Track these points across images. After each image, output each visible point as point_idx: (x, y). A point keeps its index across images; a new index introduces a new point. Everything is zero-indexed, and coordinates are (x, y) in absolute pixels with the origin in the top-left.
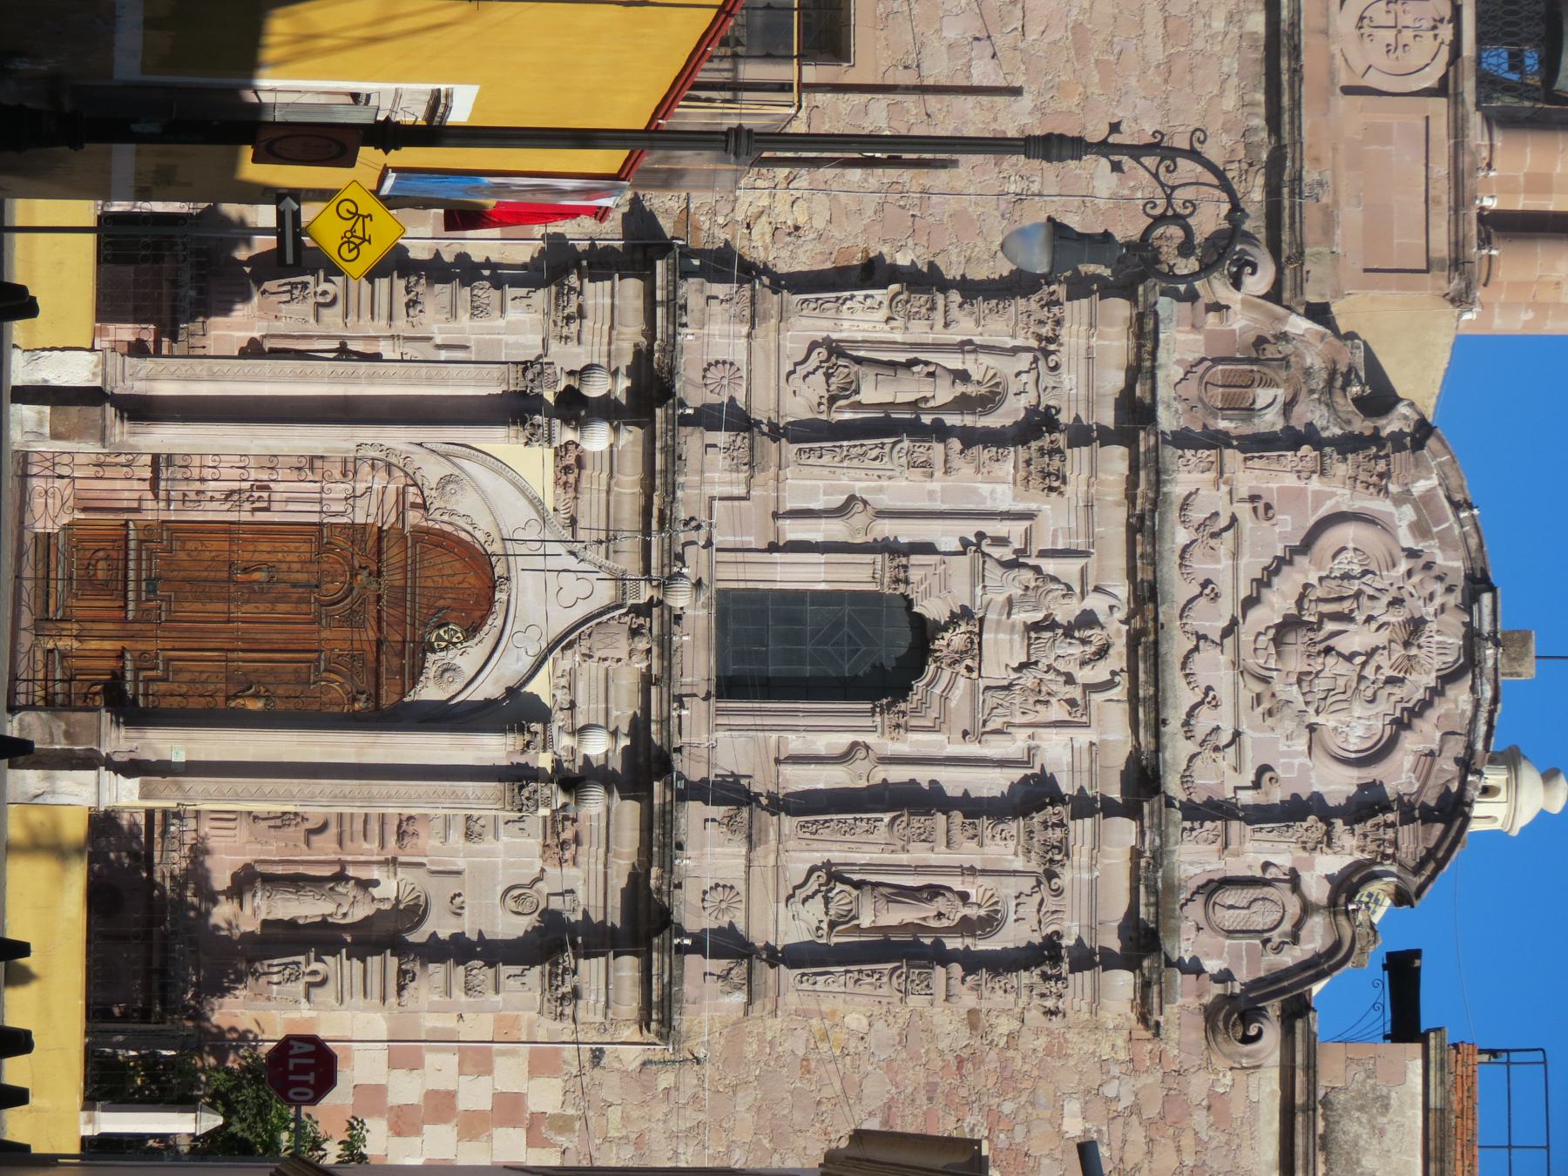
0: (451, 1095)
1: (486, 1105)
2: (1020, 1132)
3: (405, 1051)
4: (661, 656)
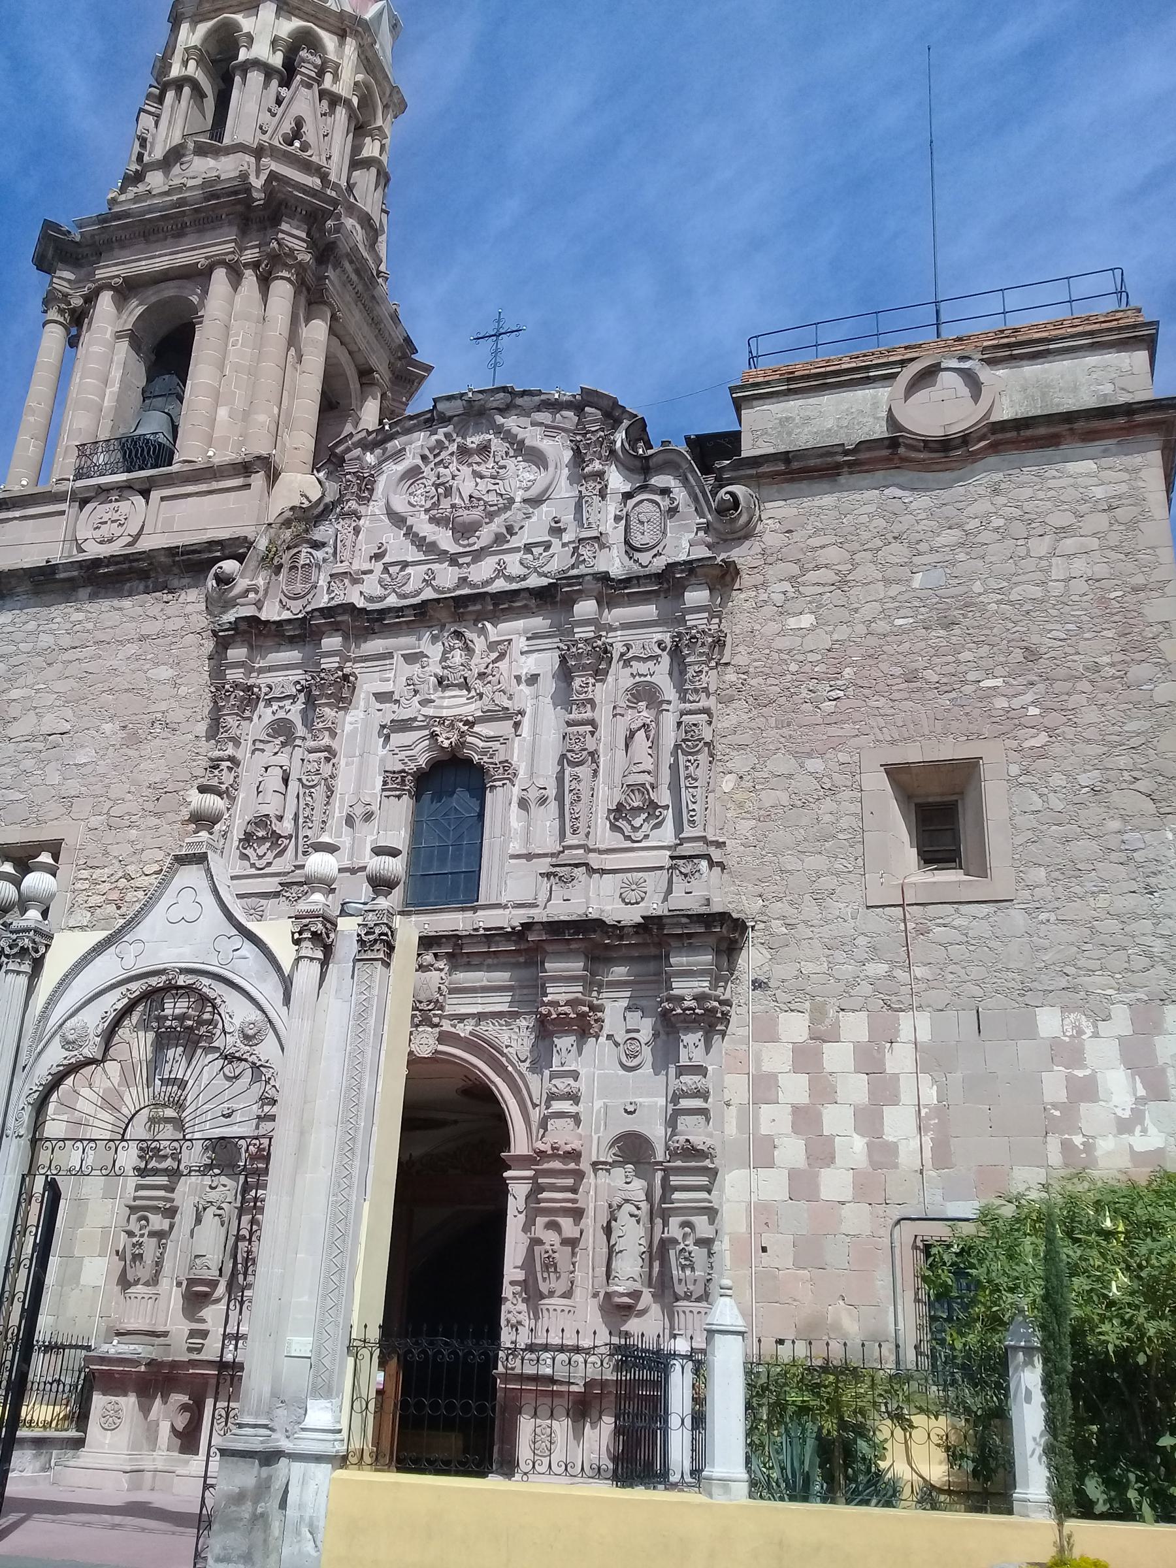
0: (796, 1110)
1: (804, 1079)
2: (812, 657)
3: (762, 1154)
4: (439, 945)
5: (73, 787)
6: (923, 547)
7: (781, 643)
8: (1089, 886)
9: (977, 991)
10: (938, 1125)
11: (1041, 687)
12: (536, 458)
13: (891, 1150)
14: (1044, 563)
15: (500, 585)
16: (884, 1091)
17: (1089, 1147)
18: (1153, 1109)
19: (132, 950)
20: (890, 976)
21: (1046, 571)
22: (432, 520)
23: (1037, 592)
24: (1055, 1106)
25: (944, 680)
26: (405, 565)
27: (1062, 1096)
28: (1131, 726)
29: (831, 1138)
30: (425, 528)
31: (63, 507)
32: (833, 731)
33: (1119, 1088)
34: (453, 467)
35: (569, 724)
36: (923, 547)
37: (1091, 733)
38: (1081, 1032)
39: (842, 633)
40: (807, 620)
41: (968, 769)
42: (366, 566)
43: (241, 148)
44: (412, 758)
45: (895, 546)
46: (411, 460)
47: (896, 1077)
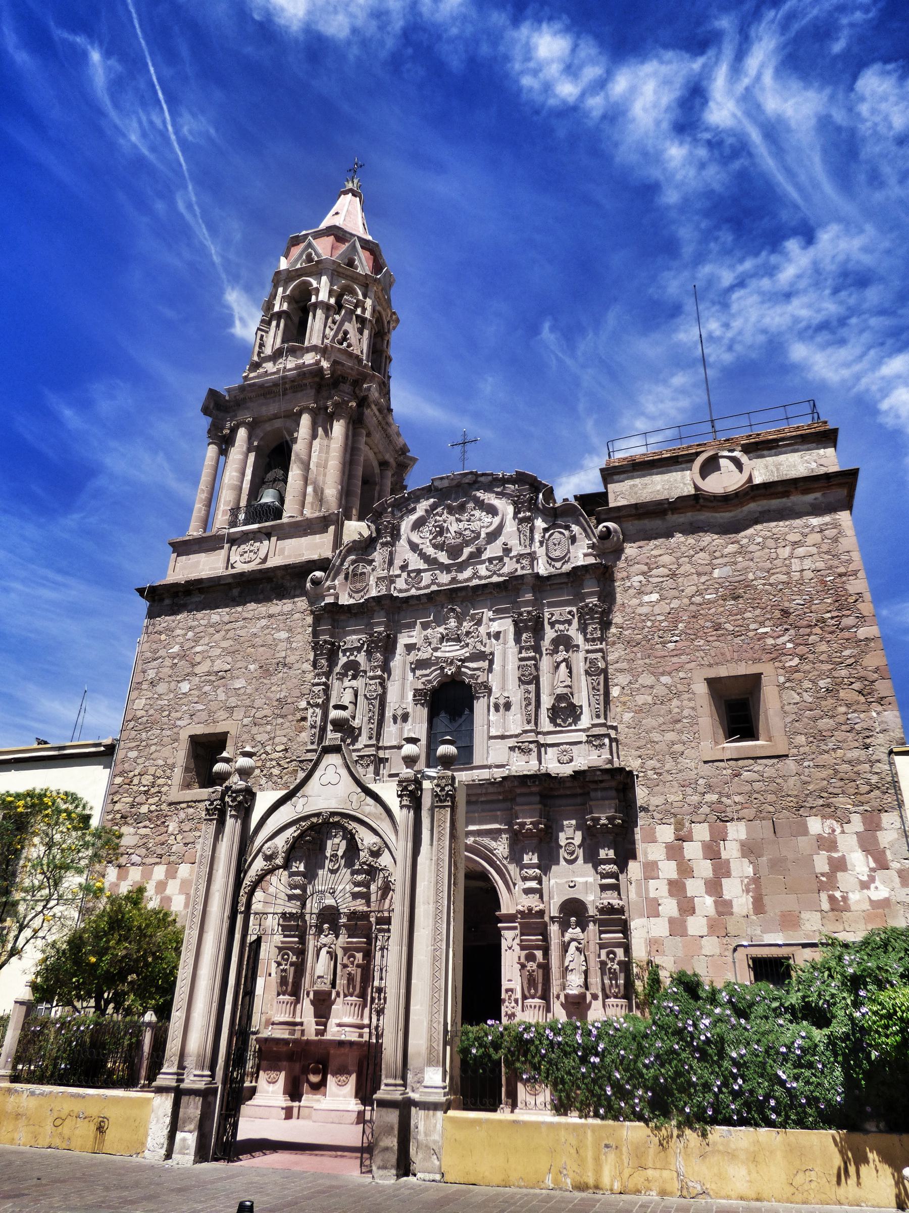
0: (671, 883)
1: (673, 864)
3: (653, 909)
5: (233, 701)
6: (717, 554)
8: (831, 745)
9: (771, 809)
10: (756, 887)
11: (792, 632)
12: (492, 511)
13: (729, 904)
14: (787, 562)
15: (476, 582)
16: (722, 870)
17: (845, 899)
18: (879, 875)
19: (302, 801)
20: (720, 802)
21: (789, 566)
22: (435, 546)
23: (784, 578)
24: (823, 875)
25: (737, 629)
27: (826, 869)
28: (847, 653)
29: (692, 899)
30: (430, 551)
32: (675, 660)
33: (860, 863)
34: (444, 517)
35: (521, 660)
36: (717, 554)
37: (823, 657)
38: (834, 831)
39: (675, 604)
40: (655, 597)
41: (755, 680)
42: (398, 572)
43: (314, 348)
44: (429, 682)
45: (702, 554)
47: (728, 862)
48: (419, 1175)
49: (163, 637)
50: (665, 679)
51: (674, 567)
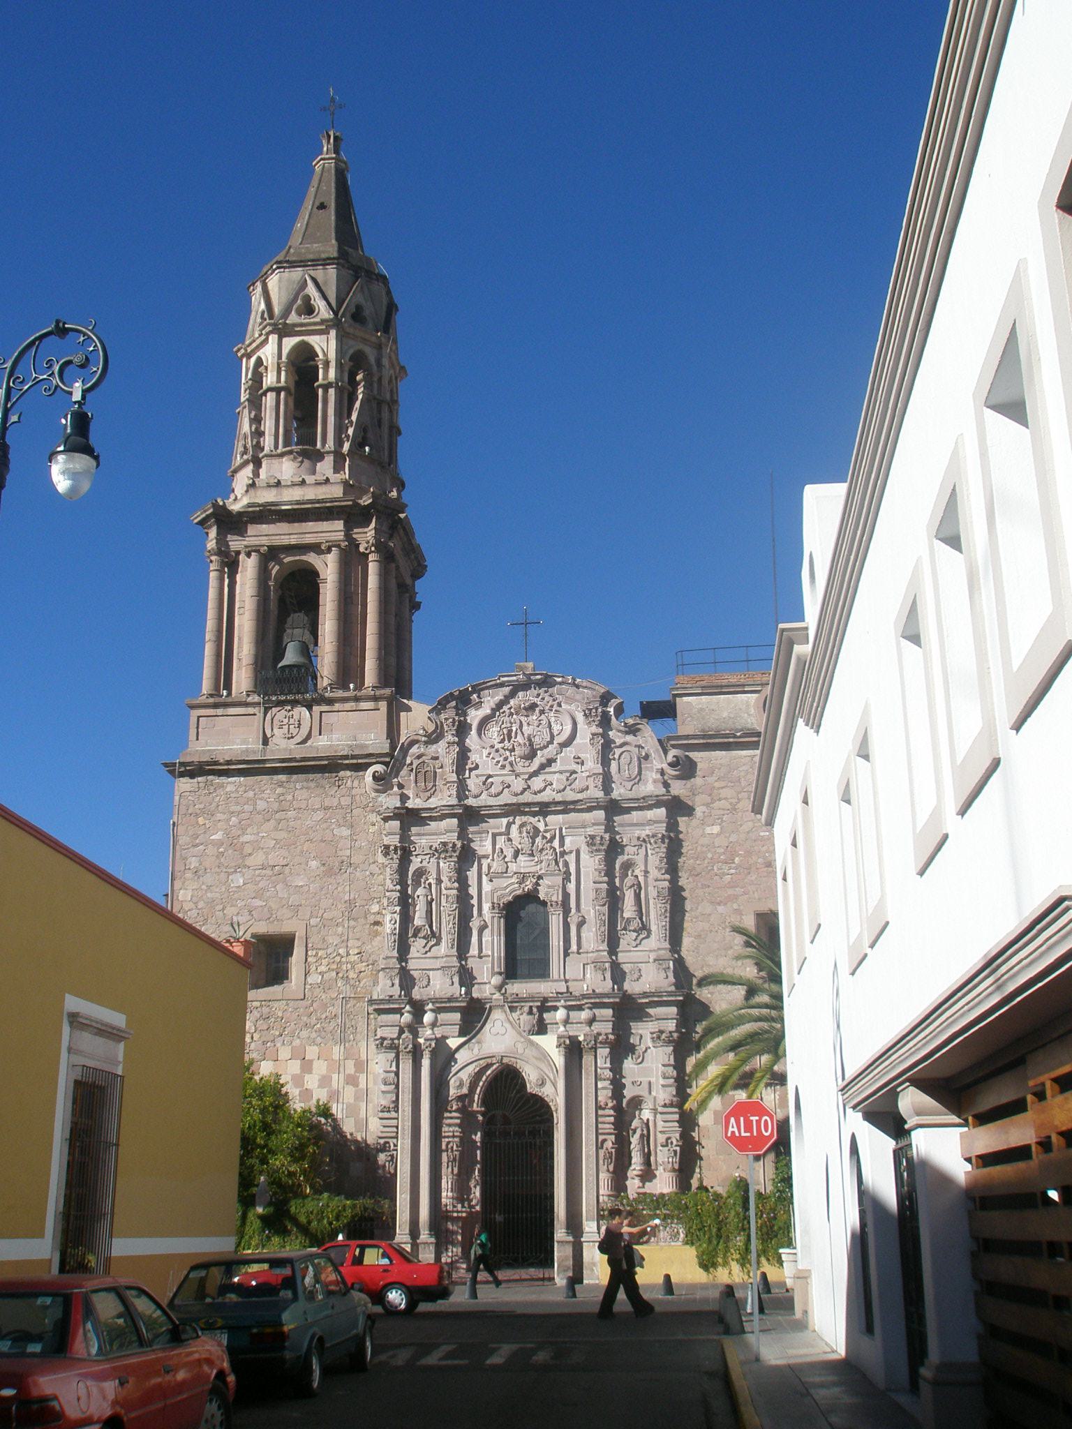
5: (294, 899)
7: (705, 841)
15: (546, 796)
26: (490, 776)
31: (251, 710)
32: (730, 892)
39: (733, 838)
40: (716, 829)
46: (486, 710)
48: (585, 1282)
49: (201, 821)
50: (720, 909)
51: (734, 801)
